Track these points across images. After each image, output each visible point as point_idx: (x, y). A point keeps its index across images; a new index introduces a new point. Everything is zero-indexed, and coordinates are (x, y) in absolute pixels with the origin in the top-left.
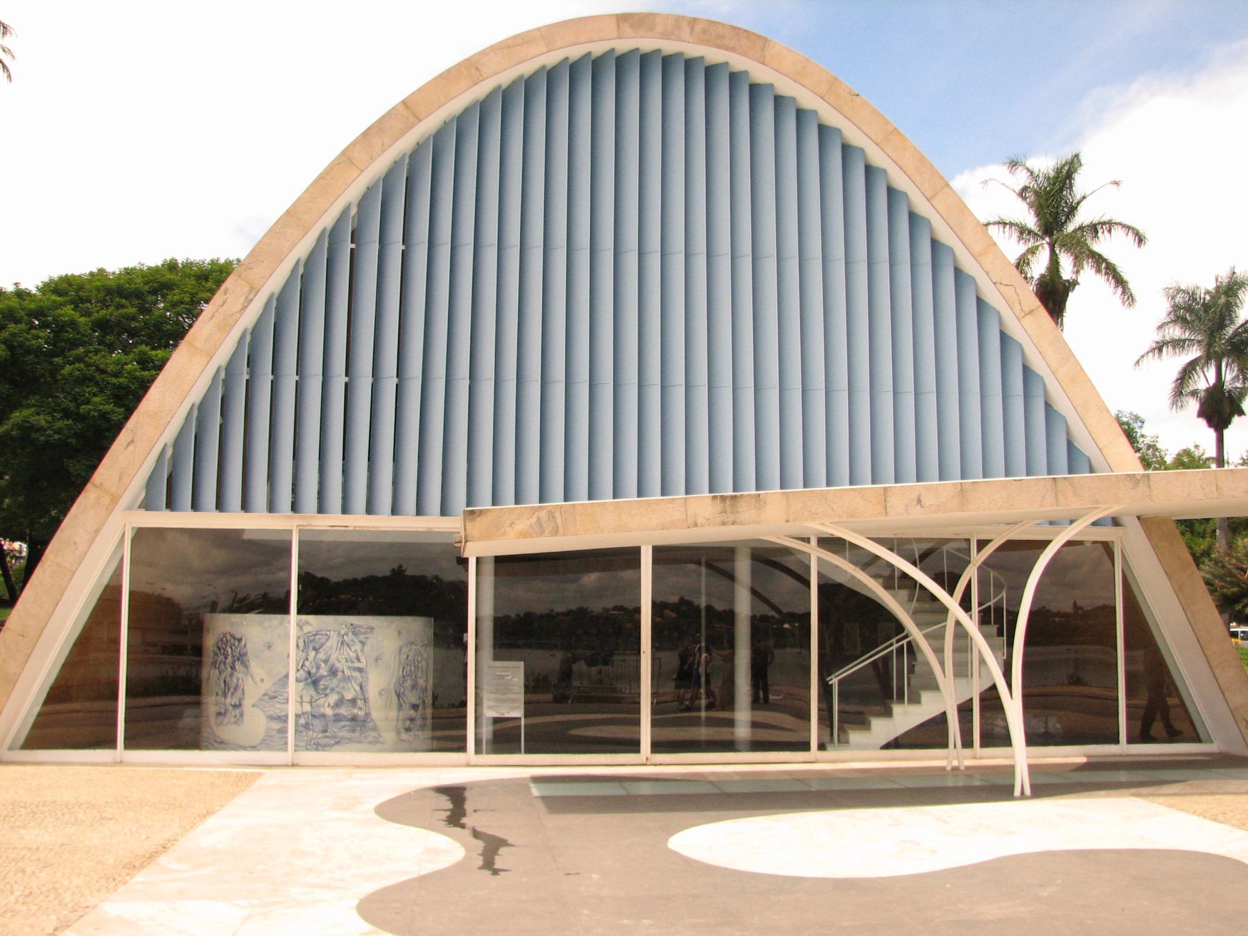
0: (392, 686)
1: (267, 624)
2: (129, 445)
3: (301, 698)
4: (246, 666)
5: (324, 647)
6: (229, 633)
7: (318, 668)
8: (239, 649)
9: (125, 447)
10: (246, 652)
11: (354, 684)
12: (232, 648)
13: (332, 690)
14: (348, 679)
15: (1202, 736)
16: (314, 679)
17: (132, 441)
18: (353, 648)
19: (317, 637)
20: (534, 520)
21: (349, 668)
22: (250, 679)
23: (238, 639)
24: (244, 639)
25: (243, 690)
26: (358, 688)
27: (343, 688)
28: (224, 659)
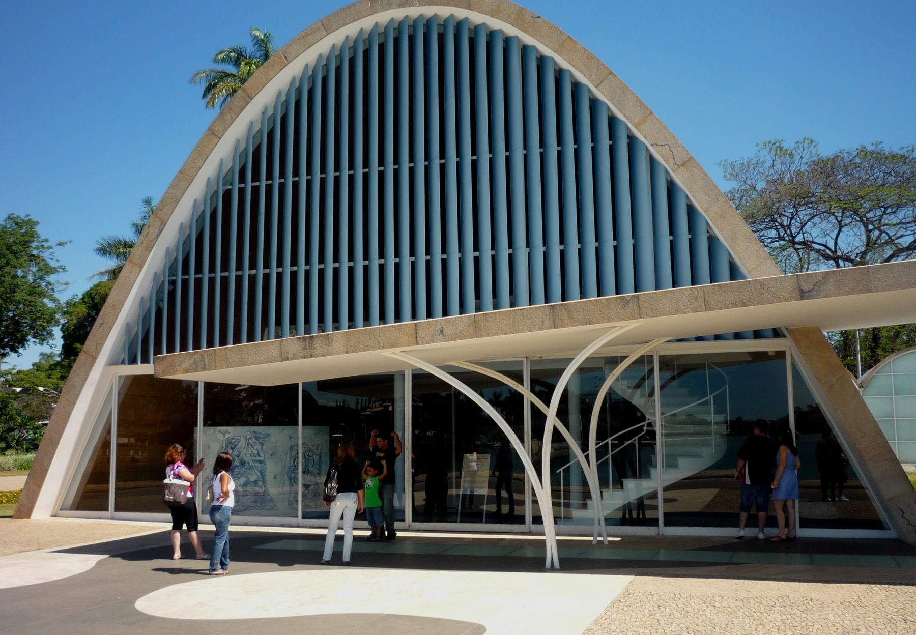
0: (284, 472)
5: (237, 447)
11: (256, 470)
13: (242, 475)
14: (251, 468)
18: (255, 448)
19: (233, 441)
21: (253, 461)
26: (259, 474)
27: (249, 473)
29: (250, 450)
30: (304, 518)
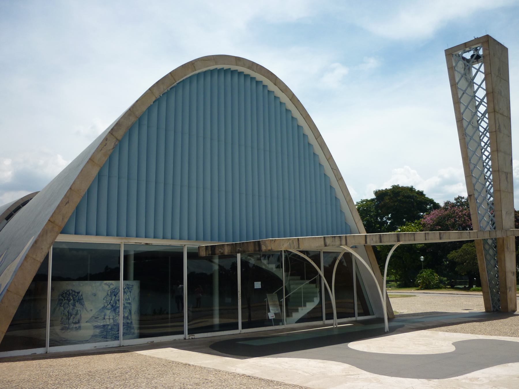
1: (94, 285)
2: (66, 204)
3: (109, 316)
4: (82, 304)
5: (118, 294)
6: (71, 290)
8: (78, 297)
9: (65, 204)
10: (82, 298)
15: (371, 313)
16: (114, 308)
17: (68, 202)
18: (128, 294)
20: (288, 243)
22: (85, 310)
23: (77, 292)
24: (81, 292)
25: (81, 315)
26: (129, 311)
29: (125, 297)
30: (243, 328)
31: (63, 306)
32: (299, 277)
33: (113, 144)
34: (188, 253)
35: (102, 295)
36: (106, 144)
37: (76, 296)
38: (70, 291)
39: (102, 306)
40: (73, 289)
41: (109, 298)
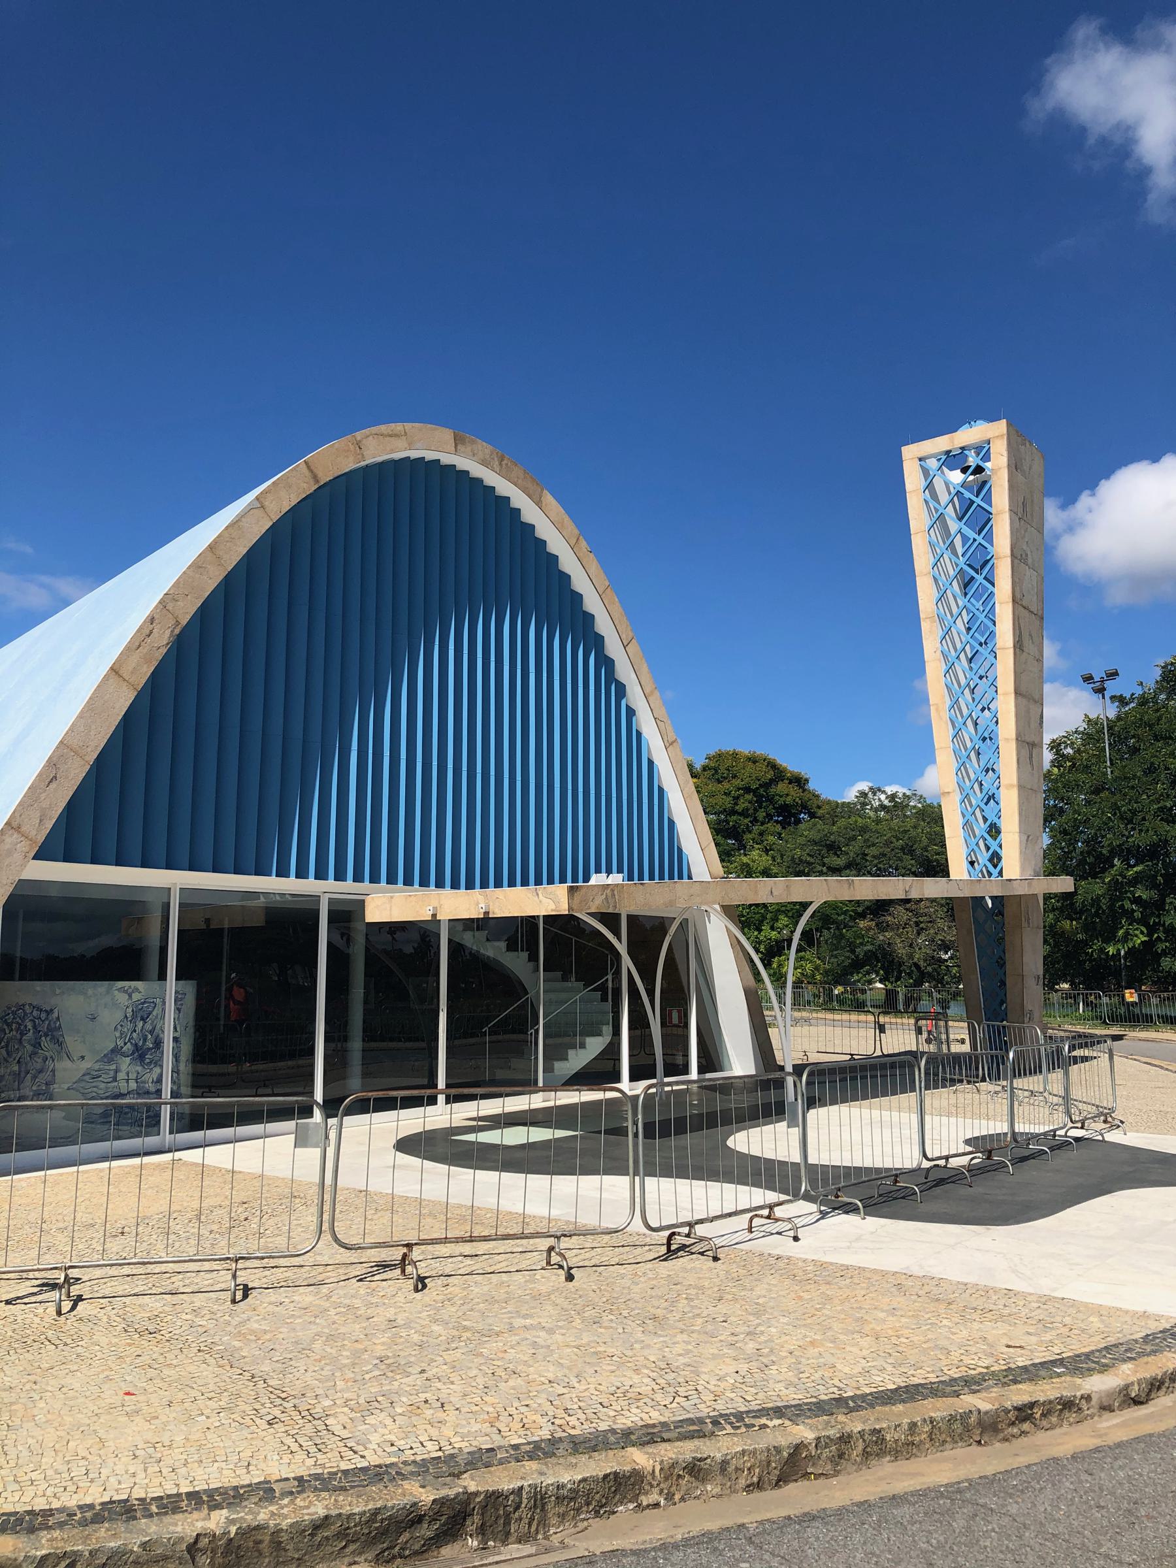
3: (128, 1074)
6: (30, 1004)
7: (145, 1040)
8: (47, 1022)
10: (60, 1026)
12: (34, 1022)
17: (55, 777)
28: (18, 1036)
31: (7, 1046)
32: (559, 974)
33: (168, 633)
34: (331, 913)
35: (110, 1017)
36: (151, 632)
37: (43, 1021)
38: (27, 1007)
39: (112, 1046)
40: (35, 1003)
41: (130, 1026)
